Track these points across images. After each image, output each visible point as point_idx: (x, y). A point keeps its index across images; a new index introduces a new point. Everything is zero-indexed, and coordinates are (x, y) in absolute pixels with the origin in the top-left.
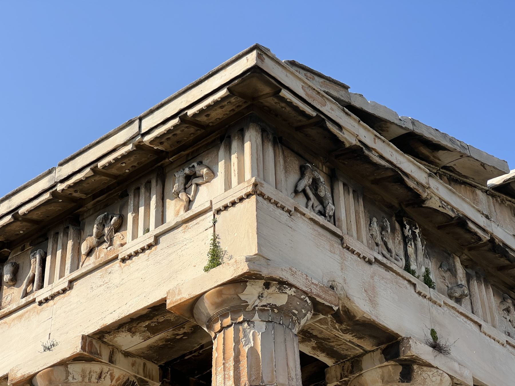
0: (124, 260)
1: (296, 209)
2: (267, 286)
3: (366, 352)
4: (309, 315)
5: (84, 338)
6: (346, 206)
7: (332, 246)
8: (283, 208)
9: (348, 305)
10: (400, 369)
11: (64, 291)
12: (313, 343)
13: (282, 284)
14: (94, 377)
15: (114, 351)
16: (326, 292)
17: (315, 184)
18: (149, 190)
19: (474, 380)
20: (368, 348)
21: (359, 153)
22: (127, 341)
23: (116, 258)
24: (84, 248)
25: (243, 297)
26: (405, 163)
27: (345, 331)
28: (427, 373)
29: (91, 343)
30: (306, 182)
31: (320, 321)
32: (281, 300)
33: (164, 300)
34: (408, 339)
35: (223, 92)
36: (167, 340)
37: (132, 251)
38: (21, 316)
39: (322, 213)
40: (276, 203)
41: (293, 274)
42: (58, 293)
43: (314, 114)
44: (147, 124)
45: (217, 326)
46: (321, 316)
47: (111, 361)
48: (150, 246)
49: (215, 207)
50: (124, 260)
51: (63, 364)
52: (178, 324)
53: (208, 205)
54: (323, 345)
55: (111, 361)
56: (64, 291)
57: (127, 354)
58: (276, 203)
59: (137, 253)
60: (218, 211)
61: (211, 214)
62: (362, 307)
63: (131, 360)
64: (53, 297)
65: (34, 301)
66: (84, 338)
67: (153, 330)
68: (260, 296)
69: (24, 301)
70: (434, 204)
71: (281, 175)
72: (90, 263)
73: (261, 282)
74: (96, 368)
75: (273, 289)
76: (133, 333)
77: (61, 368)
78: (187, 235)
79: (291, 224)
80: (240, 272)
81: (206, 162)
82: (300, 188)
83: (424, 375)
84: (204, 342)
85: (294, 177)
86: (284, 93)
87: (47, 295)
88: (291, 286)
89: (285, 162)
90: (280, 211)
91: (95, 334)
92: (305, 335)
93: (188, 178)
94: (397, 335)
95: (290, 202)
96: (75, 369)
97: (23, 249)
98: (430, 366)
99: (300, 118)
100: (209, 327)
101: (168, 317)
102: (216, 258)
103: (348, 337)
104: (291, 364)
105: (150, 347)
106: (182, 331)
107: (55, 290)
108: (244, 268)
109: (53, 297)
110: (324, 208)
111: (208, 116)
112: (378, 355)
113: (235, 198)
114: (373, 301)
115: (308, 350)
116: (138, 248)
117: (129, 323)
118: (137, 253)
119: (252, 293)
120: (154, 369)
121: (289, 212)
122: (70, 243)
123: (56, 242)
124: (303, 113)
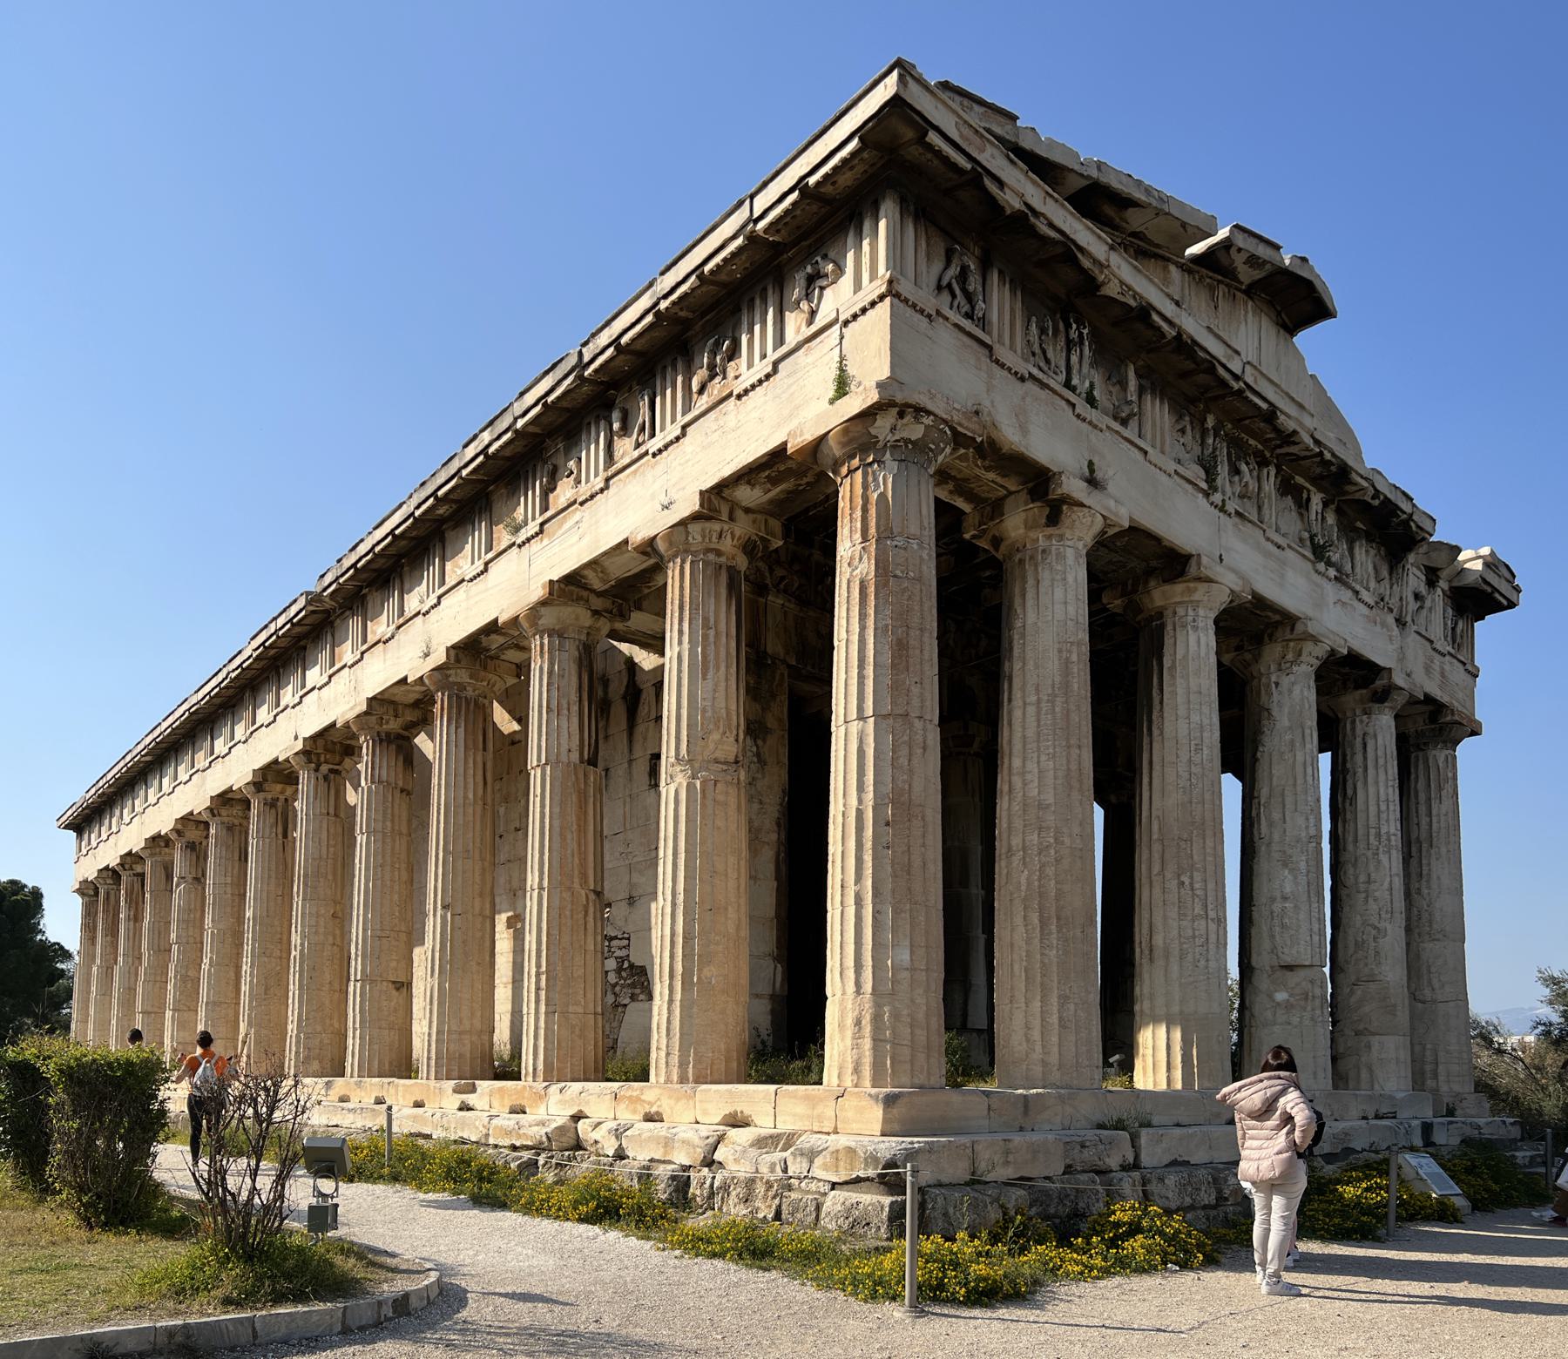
0: (739, 397)
1: (938, 312)
3: (1010, 493)
4: (948, 450)
5: (702, 493)
6: (1000, 302)
7: (978, 359)
8: (922, 312)
9: (994, 435)
10: (1047, 510)
11: (678, 439)
12: (951, 486)
14: (715, 536)
15: (734, 506)
16: (969, 419)
17: (963, 277)
19: (1131, 519)
20: (1013, 489)
22: (748, 495)
23: (730, 395)
26: (1083, 233)
27: (987, 469)
28: (1079, 513)
29: (710, 500)
31: (959, 458)
33: (785, 443)
34: (1060, 473)
36: (789, 492)
37: (747, 384)
38: (635, 472)
40: (914, 306)
41: (932, 397)
42: (672, 443)
43: (969, 166)
45: (844, 470)
46: (962, 451)
47: (731, 518)
48: (768, 377)
49: (842, 318)
50: (739, 397)
52: (799, 472)
53: (834, 315)
54: (962, 488)
55: (731, 518)
56: (678, 439)
57: (747, 510)
58: (914, 306)
59: (753, 387)
60: (846, 323)
61: (837, 327)
62: (1011, 436)
63: (752, 516)
64: (666, 447)
65: (647, 453)
66: (702, 493)
67: (774, 481)
69: (636, 454)
71: (923, 267)
72: (702, 402)
74: (716, 526)
76: (753, 486)
78: (810, 359)
79: (930, 333)
82: (945, 282)
83: (1074, 517)
84: (829, 491)
85: (938, 266)
87: (660, 445)
89: (928, 245)
90: (919, 316)
91: (712, 488)
92: (942, 476)
94: (1049, 470)
98: (1082, 505)
99: (951, 175)
100: (836, 472)
101: (790, 464)
102: (842, 386)
103: (991, 476)
104: (924, 512)
105: (771, 501)
106: (805, 480)
107: (668, 439)
108: (874, 397)
109: (666, 447)
110: (973, 308)
111: (834, 183)
112: (1024, 496)
113: (865, 303)
114: (1024, 429)
115: (944, 495)
116: (754, 380)
117: (748, 474)
118: (753, 387)
120: (776, 525)
121: (929, 316)
124: (954, 167)
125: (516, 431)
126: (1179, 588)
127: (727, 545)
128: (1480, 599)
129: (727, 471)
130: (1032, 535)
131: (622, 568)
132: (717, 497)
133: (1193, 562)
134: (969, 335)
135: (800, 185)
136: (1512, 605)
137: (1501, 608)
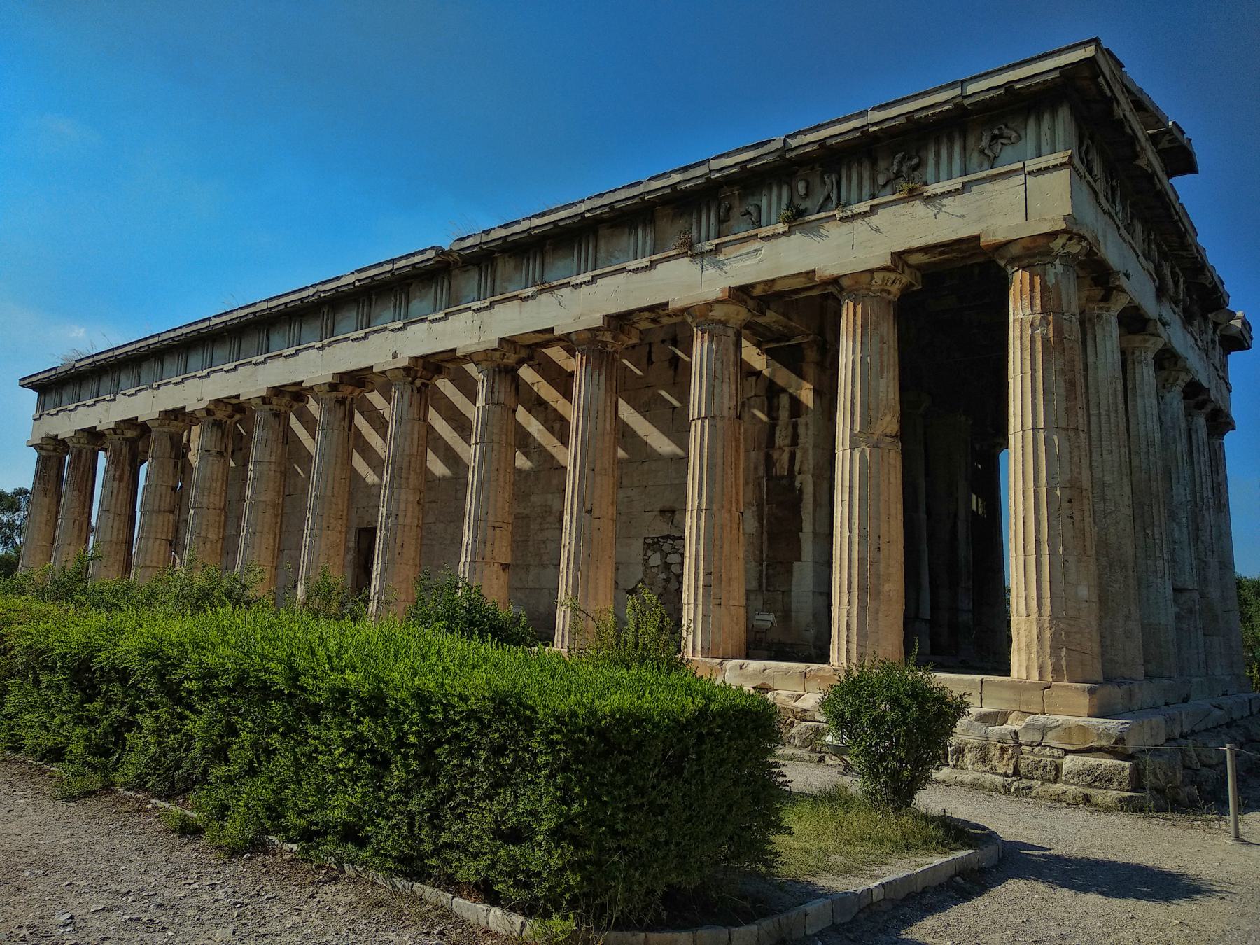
2: (1070, 239)
5: (892, 254)
10: (1103, 293)
13: (1082, 238)
18: (951, 141)
21: (1121, 124)
24: (881, 180)
25: (1051, 245)
30: (1084, 148)
32: (1075, 248)
35: (1055, 75)
39: (1090, 171)
44: (971, 89)
51: (871, 271)
57: (910, 266)
66: (892, 254)
67: (941, 253)
68: (1064, 246)
70: (1142, 162)
73: (1067, 236)
74: (893, 276)
75: (1074, 241)
77: (869, 275)
80: (1057, 228)
81: (1010, 125)
86: (1101, 80)
88: (1086, 239)
93: (994, 138)
95: (1082, 169)
96: (878, 276)
97: (812, 169)
98: (1124, 291)
118: (943, 193)
119: (1057, 244)
120: (919, 275)
122: (866, 174)
123: (849, 169)
125: (709, 179)
126: (1139, 338)
127: (895, 289)
128: (1238, 342)
129: (916, 244)
130: (1091, 305)
131: (779, 287)
132: (900, 257)
133: (1151, 324)
134: (1092, 187)
135: (1008, 86)
136: (1249, 347)
137: (1243, 348)
